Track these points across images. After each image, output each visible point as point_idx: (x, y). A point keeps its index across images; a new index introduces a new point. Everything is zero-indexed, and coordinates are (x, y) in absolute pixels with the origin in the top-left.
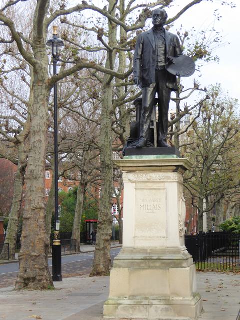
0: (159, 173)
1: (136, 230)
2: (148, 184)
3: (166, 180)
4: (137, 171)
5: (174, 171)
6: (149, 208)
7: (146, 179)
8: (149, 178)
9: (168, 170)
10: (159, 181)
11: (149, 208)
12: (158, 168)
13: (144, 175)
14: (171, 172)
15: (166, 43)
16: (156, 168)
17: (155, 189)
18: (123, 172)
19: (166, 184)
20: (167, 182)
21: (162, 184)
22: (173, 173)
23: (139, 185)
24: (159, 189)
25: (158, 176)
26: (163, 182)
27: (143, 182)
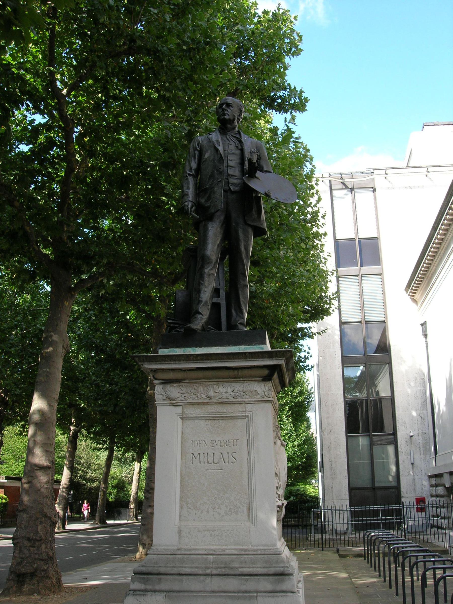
0: (233, 384)
1: (181, 507)
2: (208, 407)
3: (247, 398)
4: (185, 379)
5: (267, 378)
6: (211, 460)
7: (203, 396)
8: (212, 394)
9: (251, 377)
10: (232, 399)
11: (211, 460)
12: (231, 373)
13: (201, 389)
14: (258, 382)
15: (241, 146)
16: (227, 373)
17: (223, 418)
18: (155, 382)
19: (249, 407)
20: (249, 402)
21: (239, 408)
22: (262, 384)
23: (191, 411)
24: (233, 418)
25: (230, 390)
26: (241, 403)
27: (199, 403)
